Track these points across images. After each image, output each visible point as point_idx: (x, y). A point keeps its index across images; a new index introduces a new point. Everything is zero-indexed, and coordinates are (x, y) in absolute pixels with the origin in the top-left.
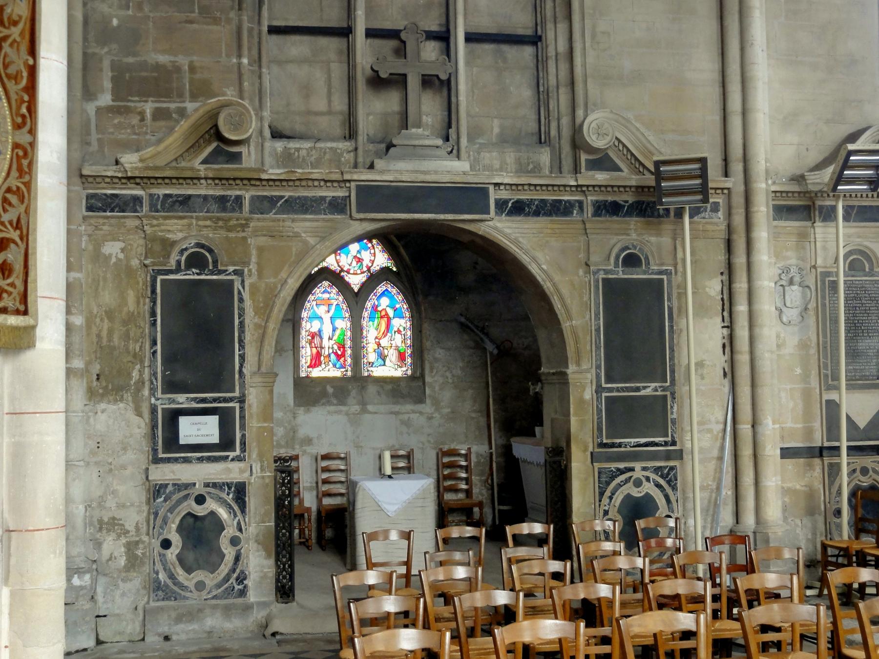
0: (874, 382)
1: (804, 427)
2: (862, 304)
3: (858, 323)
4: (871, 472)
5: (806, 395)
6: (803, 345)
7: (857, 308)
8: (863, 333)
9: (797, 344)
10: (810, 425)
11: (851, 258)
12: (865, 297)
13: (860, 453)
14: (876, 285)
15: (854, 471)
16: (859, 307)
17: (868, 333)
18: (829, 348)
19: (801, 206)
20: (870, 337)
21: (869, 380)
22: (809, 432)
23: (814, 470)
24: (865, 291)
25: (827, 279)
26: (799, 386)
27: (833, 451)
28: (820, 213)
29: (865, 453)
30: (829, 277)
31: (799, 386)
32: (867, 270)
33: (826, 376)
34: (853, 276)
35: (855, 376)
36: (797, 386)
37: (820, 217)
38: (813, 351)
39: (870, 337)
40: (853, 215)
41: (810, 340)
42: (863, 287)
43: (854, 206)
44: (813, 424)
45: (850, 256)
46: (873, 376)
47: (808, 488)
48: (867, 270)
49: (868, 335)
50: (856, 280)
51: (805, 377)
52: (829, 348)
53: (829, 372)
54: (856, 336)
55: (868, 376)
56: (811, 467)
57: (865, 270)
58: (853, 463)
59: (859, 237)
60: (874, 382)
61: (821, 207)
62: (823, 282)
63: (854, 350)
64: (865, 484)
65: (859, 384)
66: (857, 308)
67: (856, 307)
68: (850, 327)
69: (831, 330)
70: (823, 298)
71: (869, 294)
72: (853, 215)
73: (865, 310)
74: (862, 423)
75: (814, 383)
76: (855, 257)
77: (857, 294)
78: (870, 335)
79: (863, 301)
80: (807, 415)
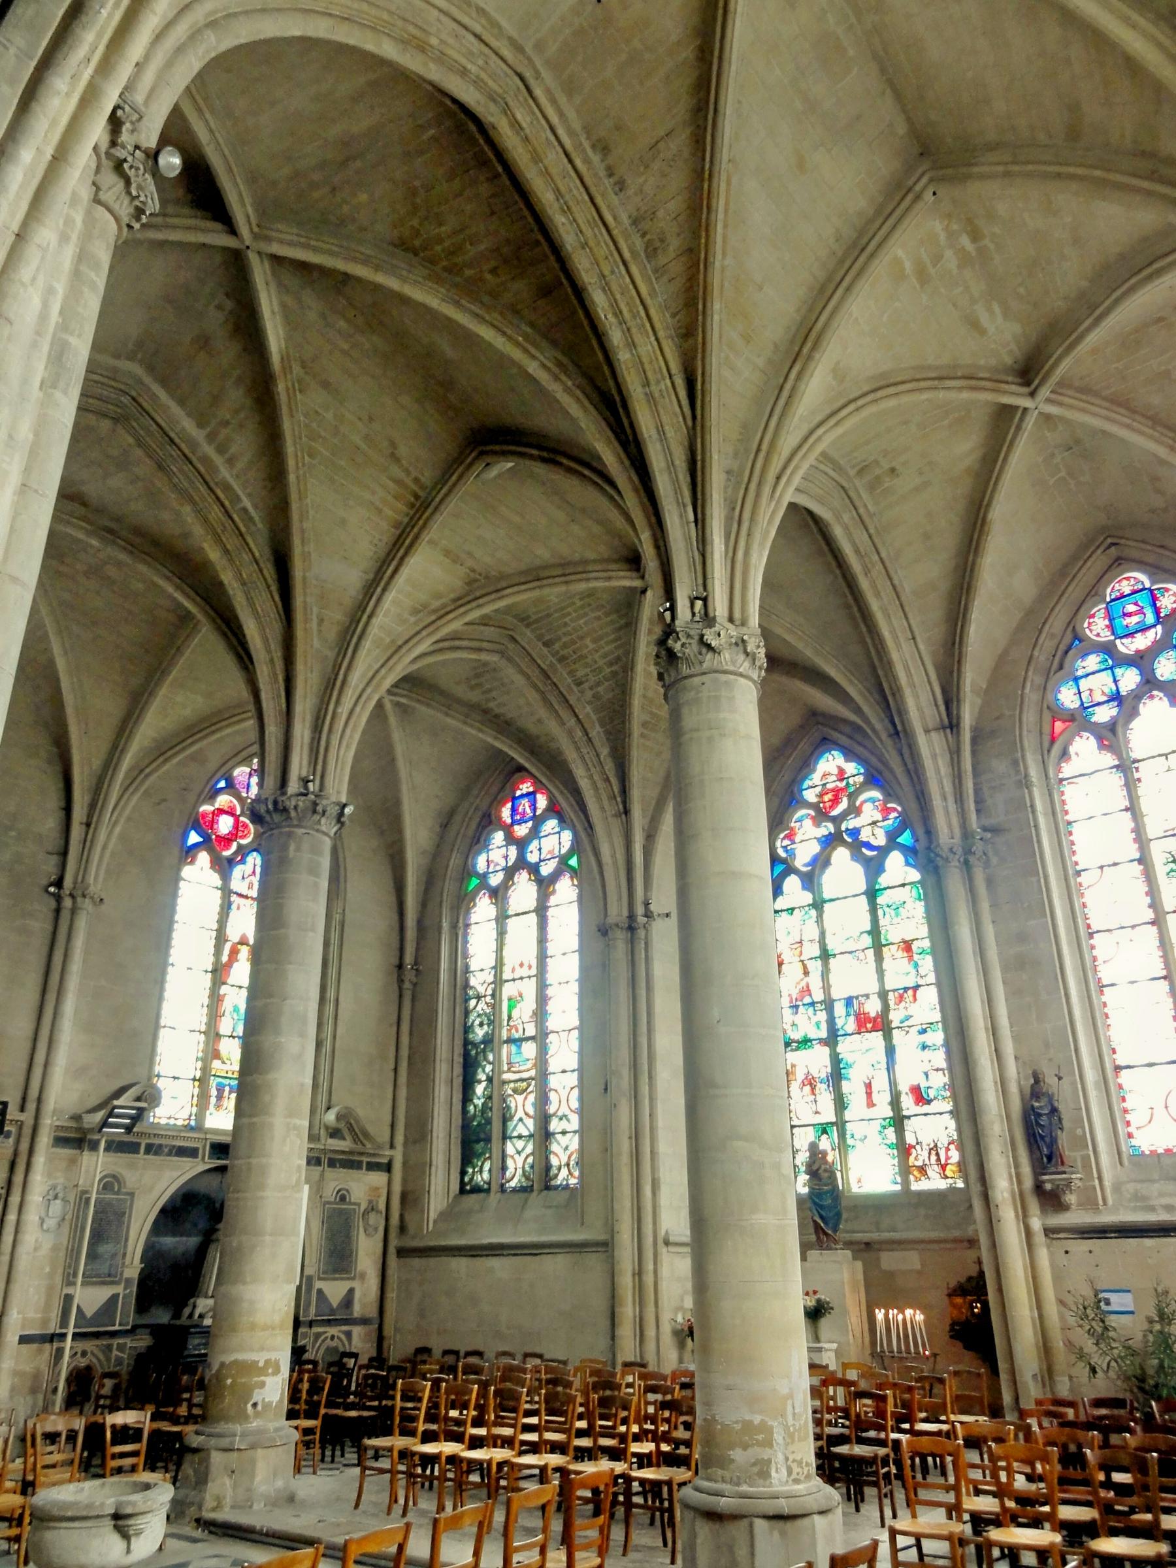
22: (45, 1322)
51: (51, 1275)
56: (40, 1351)
62: (81, 1198)
74: (89, 1313)
75: (58, 1279)
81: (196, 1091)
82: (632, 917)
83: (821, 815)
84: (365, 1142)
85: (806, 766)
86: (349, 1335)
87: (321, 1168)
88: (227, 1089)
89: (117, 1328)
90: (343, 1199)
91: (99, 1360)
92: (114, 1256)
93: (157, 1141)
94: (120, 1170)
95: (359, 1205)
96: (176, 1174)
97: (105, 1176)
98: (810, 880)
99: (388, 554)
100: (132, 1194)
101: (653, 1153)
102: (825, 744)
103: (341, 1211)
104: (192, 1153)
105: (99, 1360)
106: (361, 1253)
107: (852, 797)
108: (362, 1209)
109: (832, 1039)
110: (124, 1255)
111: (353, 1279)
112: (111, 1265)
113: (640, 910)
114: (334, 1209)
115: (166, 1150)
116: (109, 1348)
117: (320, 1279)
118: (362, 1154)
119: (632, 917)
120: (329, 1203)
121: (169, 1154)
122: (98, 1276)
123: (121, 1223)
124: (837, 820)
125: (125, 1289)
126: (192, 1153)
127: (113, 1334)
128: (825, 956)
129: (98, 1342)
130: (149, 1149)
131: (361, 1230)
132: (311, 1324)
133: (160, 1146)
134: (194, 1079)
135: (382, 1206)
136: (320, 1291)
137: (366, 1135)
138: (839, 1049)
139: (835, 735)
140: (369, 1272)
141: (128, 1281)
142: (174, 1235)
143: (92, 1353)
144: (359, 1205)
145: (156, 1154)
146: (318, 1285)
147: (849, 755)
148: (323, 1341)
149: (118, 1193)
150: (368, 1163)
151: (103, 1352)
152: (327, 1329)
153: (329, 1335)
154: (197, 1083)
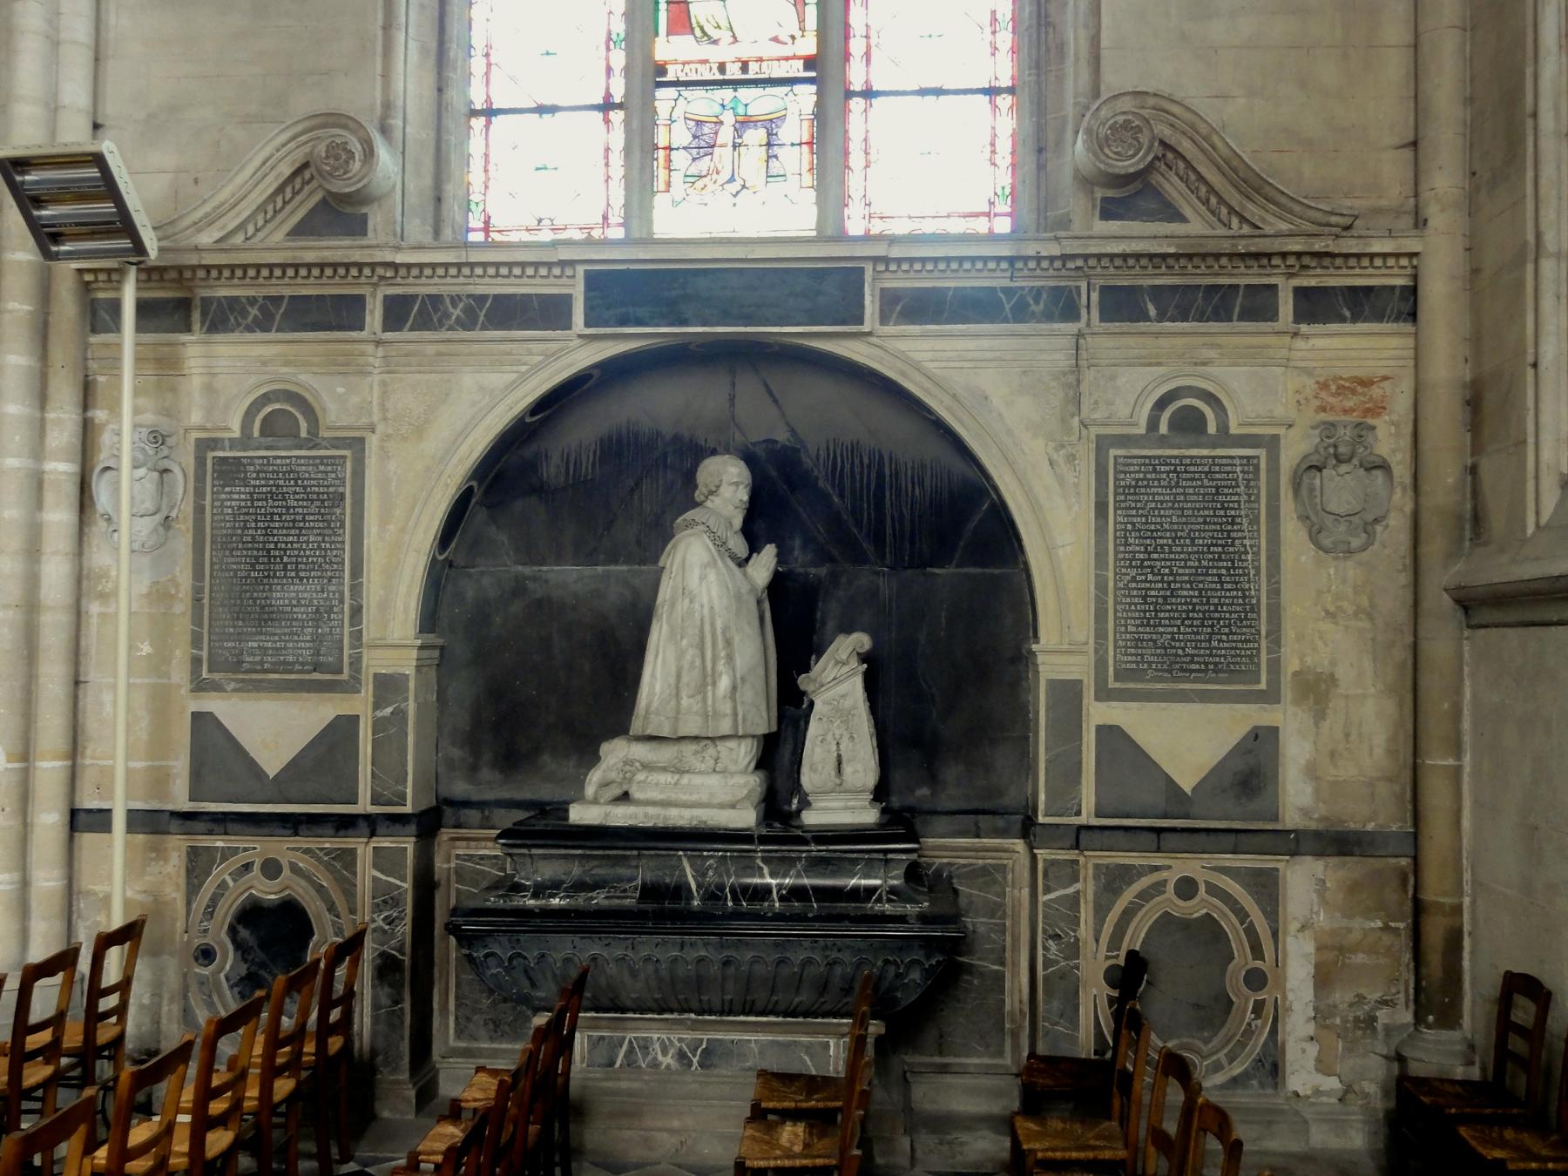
0: (307, 677)
1: (149, 768)
2: (288, 508)
3: (276, 549)
4: (286, 872)
5: (160, 701)
6: (160, 595)
7: (276, 518)
8: (285, 569)
9: (145, 590)
10: (163, 763)
11: (268, 409)
12: (295, 493)
13: (253, 830)
14: (322, 468)
15: (247, 867)
16: (280, 515)
17: (297, 570)
18: (206, 601)
19: (167, 301)
20: (301, 579)
21: (291, 672)
22: (159, 779)
23: (166, 860)
24: (296, 480)
25: (210, 455)
26: (146, 681)
27: (189, 823)
28: (204, 314)
29: (266, 831)
30: (213, 450)
31: (146, 681)
32: (303, 434)
33: (196, 662)
34: (268, 448)
35: (262, 663)
36: (139, 681)
37: (203, 323)
38: (182, 607)
39: (301, 579)
40: (278, 317)
41: (177, 586)
42: (292, 471)
43: (282, 297)
44: (171, 763)
45: (264, 405)
46: (302, 664)
47: (151, 899)
48: (303, 434)
49: (297, 576)
50: (276, 457)
51: (158, 664)
52: (206, 601)
53: (205, 654)
54: (268, 577)
55: (293, 664)
56: (159, 853)
57: (297, 436)
58: (245, 849)
59: (287, 364)
60: (307, 677)
61: (206, 302)
62: (200, 461)
63: (262, 607)
64: (273, 897)
65: (270, 681)
66: (276, 518)
67: (272, 514)
68: (257, 558)
69: (212, 564)
70: (199, 493)
71: (305, 487)
72: (278, 317)
73: (294, 521)
74: (272, 763)
75: (179, 674)
76: (277, 406)
77: (278, 486)
78: (302, 574)
79: (291, 503)
80: (158, 745)
81: (618, 138)
84: (1252, 211)
86: (1266, 887)
87: (1072, 327)
88: (728, 118)
89: (364, 805)
90: (1189, 424)
91: (320, 889)
92: (321, 615)
93: (424, 288)
94: (303, 377)
95: (1272, 443)
96: (497, 379)
97: (266, 399)
100: (358, 444)
103: (1179, 468)
104: (551, 313)
105: (320, 889)
106: (1298, 608)
108: (1290, 457)
110: (357, 611)
111: (1271, 696)
112: (317, 639)
114: (1153, 463)
115: (456, 313)
116: (348, 857)
117: (1104, 694)
118: (1260, 257)
120: (1124, 441)
121: (468, 322)
122: (286, 667)
123: (330, 526)
125: (377, 706)
126: (551, 313)
127: (345, 824)
129: (303, 842)
130: (398, 313)
131: (1292, 531)
132: (1079, 837)
133: (436, 300)
134: (607, 106)
135: (1389, 442)
136: (1111, 736)
137: (1254, 185)
140: (1344, 673)
141: (387, 686)
142: (590, 559)
143: (295, 869)
144: (1272, 443)
145: (424, 323)
146: (1098, 713)
148: (1145, 896)
149: (313, 441)
150: (1300, 292)
151: (329, 867)
152: (1157, 860)
153: (1172, 877)
154: (617, 116)
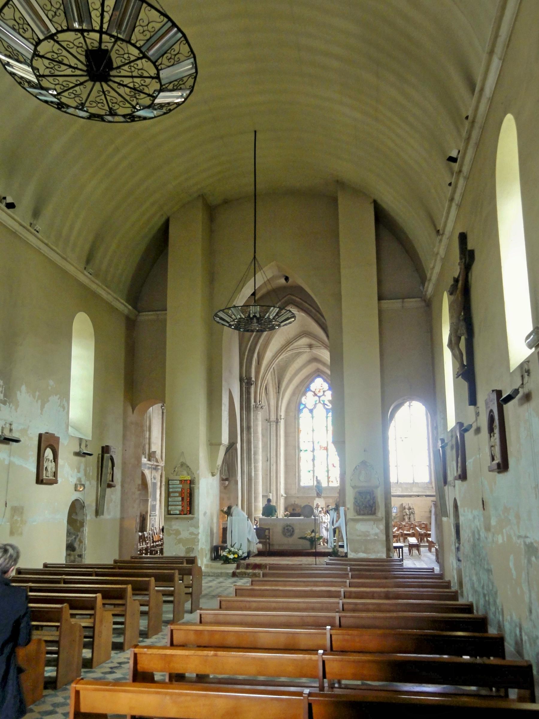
82: (277, 419)
83: (315, 395)
85: (313, 381)
98: (311, 411)
99: (279, 350)
101: (280, 476)
102: (319, 376)
107: (324, 392)
109: (314, 450)
113: (279, 418)
119: (277, 419)
124: (319, 397)
128: (313, 430)
138: (314, 453)
139: (322, 375)
147: (325, 380)
